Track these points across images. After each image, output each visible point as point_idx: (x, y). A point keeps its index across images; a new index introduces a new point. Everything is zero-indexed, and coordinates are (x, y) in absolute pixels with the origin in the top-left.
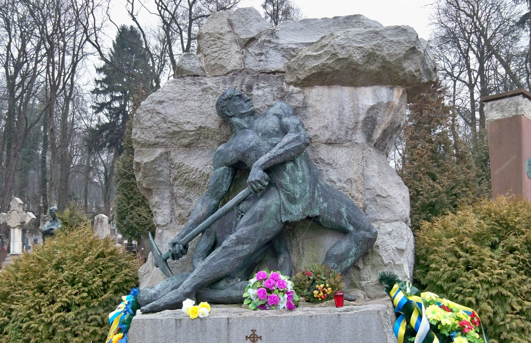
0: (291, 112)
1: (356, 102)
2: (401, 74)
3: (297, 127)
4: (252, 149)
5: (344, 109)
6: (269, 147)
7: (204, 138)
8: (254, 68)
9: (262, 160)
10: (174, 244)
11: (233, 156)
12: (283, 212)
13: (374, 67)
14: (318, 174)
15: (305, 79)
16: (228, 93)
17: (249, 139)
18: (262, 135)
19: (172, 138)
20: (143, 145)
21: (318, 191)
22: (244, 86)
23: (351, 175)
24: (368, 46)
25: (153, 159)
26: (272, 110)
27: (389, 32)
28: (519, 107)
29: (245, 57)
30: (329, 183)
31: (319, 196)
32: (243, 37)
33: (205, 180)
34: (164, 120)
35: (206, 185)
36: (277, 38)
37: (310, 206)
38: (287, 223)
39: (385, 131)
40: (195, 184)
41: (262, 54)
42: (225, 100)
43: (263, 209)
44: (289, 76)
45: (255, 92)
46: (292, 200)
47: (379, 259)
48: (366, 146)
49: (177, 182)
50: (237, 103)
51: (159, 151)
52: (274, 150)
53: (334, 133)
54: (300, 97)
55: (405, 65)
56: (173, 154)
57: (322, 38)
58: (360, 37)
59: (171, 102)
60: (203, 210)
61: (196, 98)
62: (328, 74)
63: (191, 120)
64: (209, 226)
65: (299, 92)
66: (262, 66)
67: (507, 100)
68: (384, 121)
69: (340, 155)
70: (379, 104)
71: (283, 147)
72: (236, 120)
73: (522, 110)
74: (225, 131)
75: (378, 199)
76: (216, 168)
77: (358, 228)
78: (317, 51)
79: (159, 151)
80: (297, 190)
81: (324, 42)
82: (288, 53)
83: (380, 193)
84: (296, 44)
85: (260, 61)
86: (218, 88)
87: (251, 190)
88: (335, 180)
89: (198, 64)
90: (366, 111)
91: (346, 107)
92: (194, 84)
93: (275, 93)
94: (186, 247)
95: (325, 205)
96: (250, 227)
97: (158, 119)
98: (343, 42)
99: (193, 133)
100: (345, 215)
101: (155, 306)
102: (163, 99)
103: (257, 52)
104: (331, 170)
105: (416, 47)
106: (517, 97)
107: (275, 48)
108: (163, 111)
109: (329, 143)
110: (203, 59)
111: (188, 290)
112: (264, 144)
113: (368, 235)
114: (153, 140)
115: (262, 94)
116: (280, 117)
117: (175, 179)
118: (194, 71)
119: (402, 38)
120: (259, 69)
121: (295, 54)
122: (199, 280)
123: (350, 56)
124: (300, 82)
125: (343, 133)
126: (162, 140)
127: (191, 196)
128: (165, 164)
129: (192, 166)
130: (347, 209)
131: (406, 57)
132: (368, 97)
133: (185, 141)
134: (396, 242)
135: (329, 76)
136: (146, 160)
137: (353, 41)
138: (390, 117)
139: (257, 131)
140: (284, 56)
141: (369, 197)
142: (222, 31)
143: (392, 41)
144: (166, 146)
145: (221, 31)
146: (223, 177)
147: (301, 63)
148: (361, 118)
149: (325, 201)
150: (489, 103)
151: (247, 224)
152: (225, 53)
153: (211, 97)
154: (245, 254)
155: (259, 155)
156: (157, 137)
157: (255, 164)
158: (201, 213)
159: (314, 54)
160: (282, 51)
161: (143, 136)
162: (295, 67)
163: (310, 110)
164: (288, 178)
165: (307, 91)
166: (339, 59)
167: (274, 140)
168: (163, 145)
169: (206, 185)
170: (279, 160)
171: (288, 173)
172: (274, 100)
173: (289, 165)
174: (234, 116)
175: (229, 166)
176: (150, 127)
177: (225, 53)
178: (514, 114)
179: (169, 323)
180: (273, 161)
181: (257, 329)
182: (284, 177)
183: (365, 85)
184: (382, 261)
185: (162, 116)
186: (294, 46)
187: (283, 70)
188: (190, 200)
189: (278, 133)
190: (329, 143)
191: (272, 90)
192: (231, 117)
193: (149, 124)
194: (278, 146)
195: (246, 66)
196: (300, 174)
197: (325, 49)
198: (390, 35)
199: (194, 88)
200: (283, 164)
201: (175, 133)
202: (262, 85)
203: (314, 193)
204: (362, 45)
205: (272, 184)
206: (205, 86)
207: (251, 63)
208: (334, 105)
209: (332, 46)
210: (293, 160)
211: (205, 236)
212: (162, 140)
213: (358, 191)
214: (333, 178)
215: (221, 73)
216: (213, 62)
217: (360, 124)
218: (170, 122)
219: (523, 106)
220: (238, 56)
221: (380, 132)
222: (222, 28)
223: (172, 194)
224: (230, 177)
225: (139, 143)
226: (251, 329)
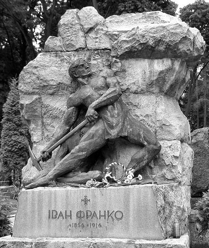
0: (112, 75)
2: (178, 52)
3: (115, 85)
4: (89, 97)
6: (97, 96)
7: (62, 89)
9: (94, 104)
10: (44, 152)
11: (78, 101)
12: (106, 134)
14: (127, 112)
16: (76, 63)
17: (88, 91)
19: (42, 89)
20: (25, 94)
21: (127, 122)
23: (149, 113)
24: (158, 36)
26: (101, 74)
30: (134, 117)
32: (86, 27)
34: (38, 78)
37: (121, 130)
38: (108, 139)
39: (171, 86)
41: (97, 38)
43: (94, 132)
44: (113, 52)
45: (93, 62)
47: (163, 162)
49: (45, 116)
50: (81, 70)
51: (35, 97)
52: (101, 98)
53: (139, 87)
55: (180, 46)
56: (43, 99)
57: (133, 29)
62: (135, 52)
64: (64, 142)
66: (97, 46)
68: (171, 79)
69: (144, 100)
72: (80, 79)
75: (164, 127)
76: (68, 108)
77: (149, 143)
79: (35, 97)
80: (114, 121)
82: (112, 37)
84: (118, 31)
89: (58, 44)
90: (158, 74)
91: (146, 71)
93: (104, 63)
94: (50, 154)
95: (131, 130)
97: (34, 77)
101: (32, 185)
103: (94, 37)
105: (187, 36)
107: (105, 34)
108: (37, 73)
109: (136, 93)
111: (51, 177)
112: (96, 95)
113: (155, 147)
114: (31, 90)
115: (97, 63)
116: (105, 78)
117: (45, 114)
118: (56, 48)
119: (178, 31)
122: (58, 172)
123: (147, 42)
125: (145, 87)
126: (37, 91)
127: (54, 124)
128: (39, 105)
131: (180, 42)
132: (159, 66)
133: (51, 91)
134: (174, 152)
135: (136, 53)
136: (27, 102)
138: (174, 77)
140: (110, 39)
142: (74, 23)
144: (39, 94)
146: (73, 113)
151: (85, 140)
156: (34, 89)
159: (128, 39)
162: (116, 47)
164: (109, 114)
167: (101, 92)
170: (104, 104)
171: (109, 112)
173: (110, 107)
175: (76, 107)
176: (29, 83)
179: (40, 193)
181: (88, 196)
182: (107, 115)
184: (165, 163)
185: (37, 76)
186: (117, 33)
187: (110, 48)
188: (53, 127)
189: (104, 87)
190: (136, 93)
191: (102, 61)
193: (29, 81)
198: (172, 29)
200: (106, 106)
201: (44, 86)
202: (97, 58)
203: (124, 123)
204: (154, 35)
205: (99, 118)
206: (63, 58)
210: (112, 104)
211: (62, 148)
212: (37, 91)
213: (152, 122)
214: (138, 114)
215: (72, 49)
216: (67, 43)
221: (168, 86)
223: (43, 123)
224: (76, 113)
225: (22, 92)
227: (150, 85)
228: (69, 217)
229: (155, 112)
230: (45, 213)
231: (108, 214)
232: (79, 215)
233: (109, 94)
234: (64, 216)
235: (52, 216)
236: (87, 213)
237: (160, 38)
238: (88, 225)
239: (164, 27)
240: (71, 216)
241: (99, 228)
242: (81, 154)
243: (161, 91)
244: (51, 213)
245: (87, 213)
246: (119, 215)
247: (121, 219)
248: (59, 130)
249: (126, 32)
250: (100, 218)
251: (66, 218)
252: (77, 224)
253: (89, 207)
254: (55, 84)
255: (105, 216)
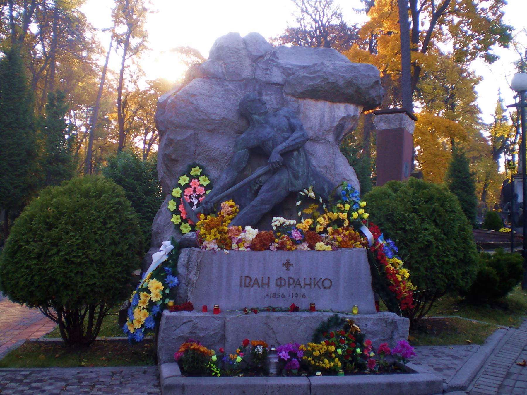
1: (333, 113)
5: (324, 117)
6: (282, 139)
8: (262, 79)
9: (281, 147)
11: (254, 143)
12: (290, 185)
13: (351, 91)
15: (303, 93)
18: (277, 130)
22: (256, 92)
23: (326, 163)
24: (348, 76)
25: (184, 138)
26: (281, 112)
27: (362, 68)
28: (403, 122)
29: (255, 69)
31: (311, 176)
32: (254, 53)
33: (223, 158)
35: (223, 162)
36: (277, 58)
40: (214, 160)
41: (267, 69)
42: (249, 101)
46: (296, 177)
48: (334, 143)
49: (200, 157)
51: (190, 133)
52: (288, 142)
53: (315, 133)
54: (296, 105)
55: (371, 92)
58: (344, 69)
59: (201, 96)
60: (228, 179)
61: (220, 96)
63: (216, 112)
65: (295, 101)
66: (268, 78)
67: (394, 115)
70: (348, 115)
71: (294, 140)
73: (405, 124)
74: (243, 123)
78: (311, 74)
79: (190, 133)
81: (317, 68)
83: (346, 178)
84: (292, 65)
85: (267, 74)
86: (237, 90)
87: (271, 168)
88: (316, 166)
91: (326, 116)
92: (219, 85)
96: (270, 194)
98: (333, 71)
99: (217, 122)
100: (327, 190)
102: (195, 93)
103: (264, 67)
104: (313, 159)
106: (401, 114)
108: (196, 103)
110: (223, 66)
117: (199, 155)
119: (371, 74)
120: (264, 79)
121: (291, 72)
123: (337, 81)
124: (297, 94)
125: (321, 133)
126: (193, 124)
129: (214, 146)
130: (328, 187)
131: (372, 87)
132: (342, 110)
133: (210, 127)
136: (179, 138)
137: (339, 71)
139: (272, 127)
140: (282, 73)
141: (338, 179)
143: (364, 75)
145: (238, 47)
147: (299, 81)
148: (335, 124)
149: (314, 179)
150: (379, 116)
151: (268, 191)
152: (241, 64)
153: (231, 97)
154: (266, 211)
155: (275, 145)
157: (274, 150)
158: (226, 181)
160: (281, 69)
161: (177, 119)
163: (301, 115)
164: (294, 162)
165: (300, 101)
166: (329, 82)
168: (192, 128)
169: (223, 162)
170: (291, 149)
172: (277, 105)
173: (295, 153)
174: (255, 114)
176: (184, 113)
177: (241, 64)
178: (398, 126)
180: (287, 149)
183: (340, 102)
186: (290, 67)
187: (282, 83)
191: (276, 97)
192: (252, 114)
194: (291, 139)
195: (256, 77)
196: (302, 159)
197: (318, 74)
199: (218, 88)
200: (291, 152)
201: (203, 120)
202: (269, 93)
204: (344, 75)
206: (226, 87)
207: (259, 73)
208: (318, 113)
209: (324, 72)
210: (298, 150)
217: (333, 129)
218: (201, 112)
219: (405, 121)
220: (250, 68)
222: (239, 45)
224: (248, 157)
226: (286, 259)
227: (327, 131)
228: (267, 286)
229: (334, 164)
230: (236, 280)
231: (314, 283)
232: (279, 283)
233: (297, 138)
234: (260, 283)
235: (245, 284)
236: (289, 281)
237: (350, 79)
238: (289, 296)
239: (355, 67)
240: (268, 284)
241: (303, 299)
242: (263, 207)
243: (337, 139)
244: (243, 280)
245: (289, 281)
246: (327, 284)
247: (329, 288)
248: (224, 176)
249: (304, 67)
250: (304, 288)
251: (262, 286)
252: (277, 293)
253: (292, 273)
254: (217, 118)
255: (310, 285)
